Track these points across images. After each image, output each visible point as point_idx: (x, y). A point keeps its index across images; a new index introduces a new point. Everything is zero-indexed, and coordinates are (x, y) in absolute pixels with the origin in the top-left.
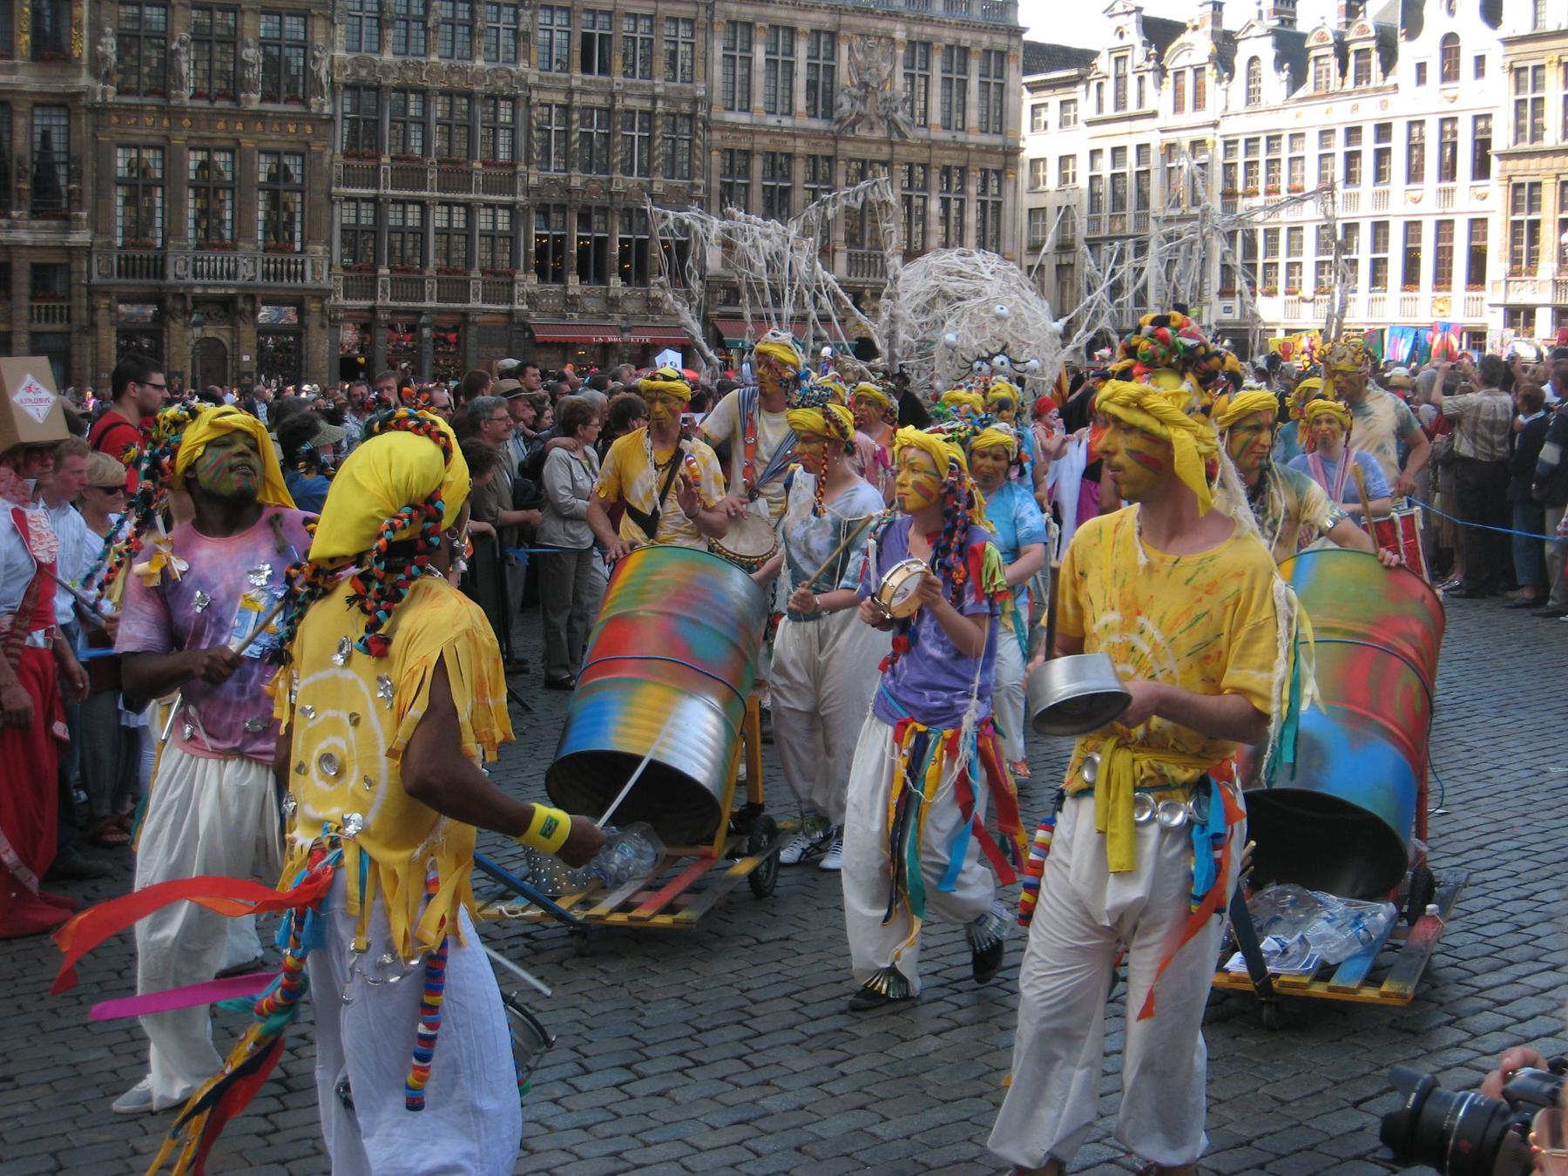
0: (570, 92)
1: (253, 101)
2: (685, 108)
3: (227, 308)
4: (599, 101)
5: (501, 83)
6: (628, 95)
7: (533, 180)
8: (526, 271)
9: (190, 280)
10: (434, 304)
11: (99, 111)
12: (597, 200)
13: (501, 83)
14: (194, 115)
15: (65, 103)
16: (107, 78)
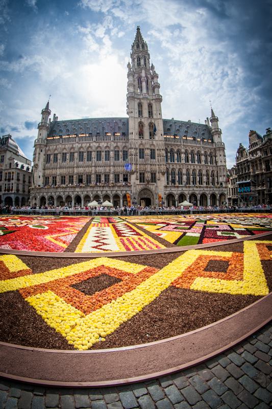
11: (265, 174)
15: (262, 174)
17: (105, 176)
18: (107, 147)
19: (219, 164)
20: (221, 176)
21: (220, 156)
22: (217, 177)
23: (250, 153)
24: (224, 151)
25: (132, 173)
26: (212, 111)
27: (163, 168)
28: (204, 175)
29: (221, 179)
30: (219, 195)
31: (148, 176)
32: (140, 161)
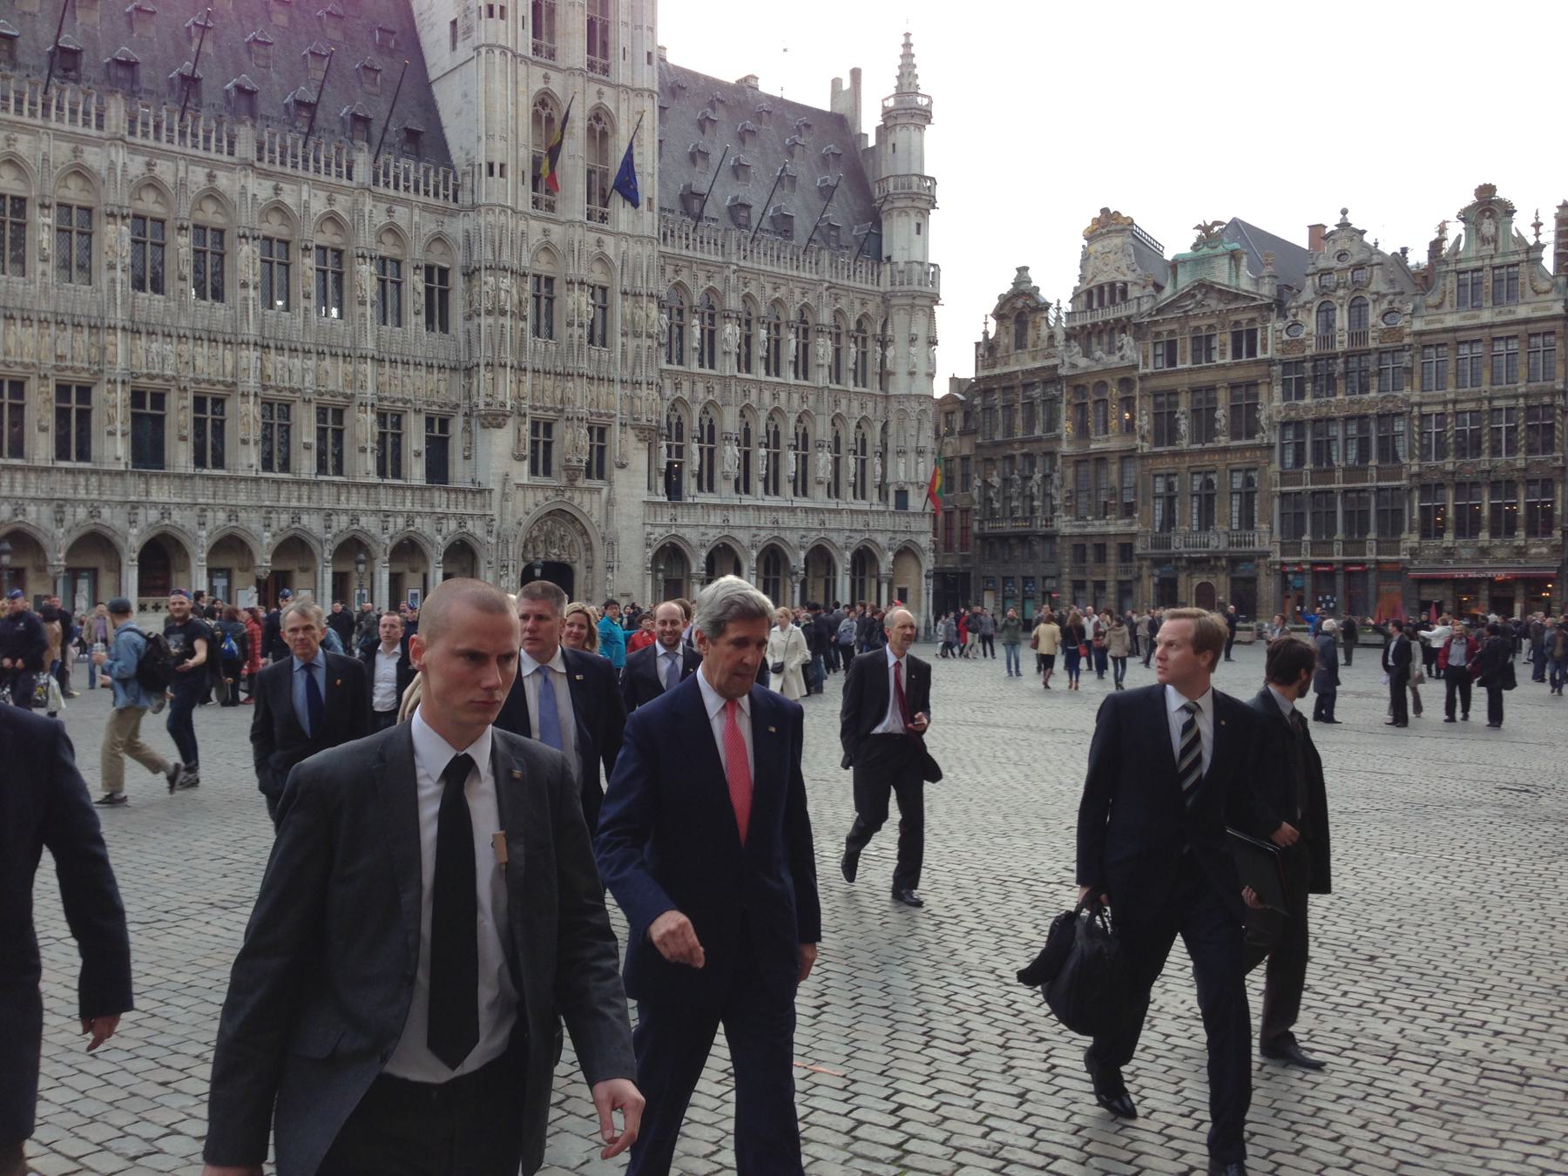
0: (1445, 403)
1: (1223, 441)
2: (1547, 400)
3: (1197, 564)
4: (1472, 406)
5: (1390, 405)
6: (1490, 400)
7: (1415, 469)
8: (1411, 531)
9: (1182, 549)
10: (1341, 558)
11: (1143, 457)
12: (1467, 477)
13: (1390, 405)
14: (1191, 453)
16: (1143, 438)
17: (322, 412)
18: (332, 218)
19: (899, 385)
20: (901, 452)
21: (913, 340)
22: (883, 456)
23: (1070, 335)
24: (931, 316)
25: (495, 419)
26: (907, 45)
27: (651, 405)
28: (820, 445)
29: (900, 471)
30: (890, 556)
31: (571, 442)
32: (537, 351)
